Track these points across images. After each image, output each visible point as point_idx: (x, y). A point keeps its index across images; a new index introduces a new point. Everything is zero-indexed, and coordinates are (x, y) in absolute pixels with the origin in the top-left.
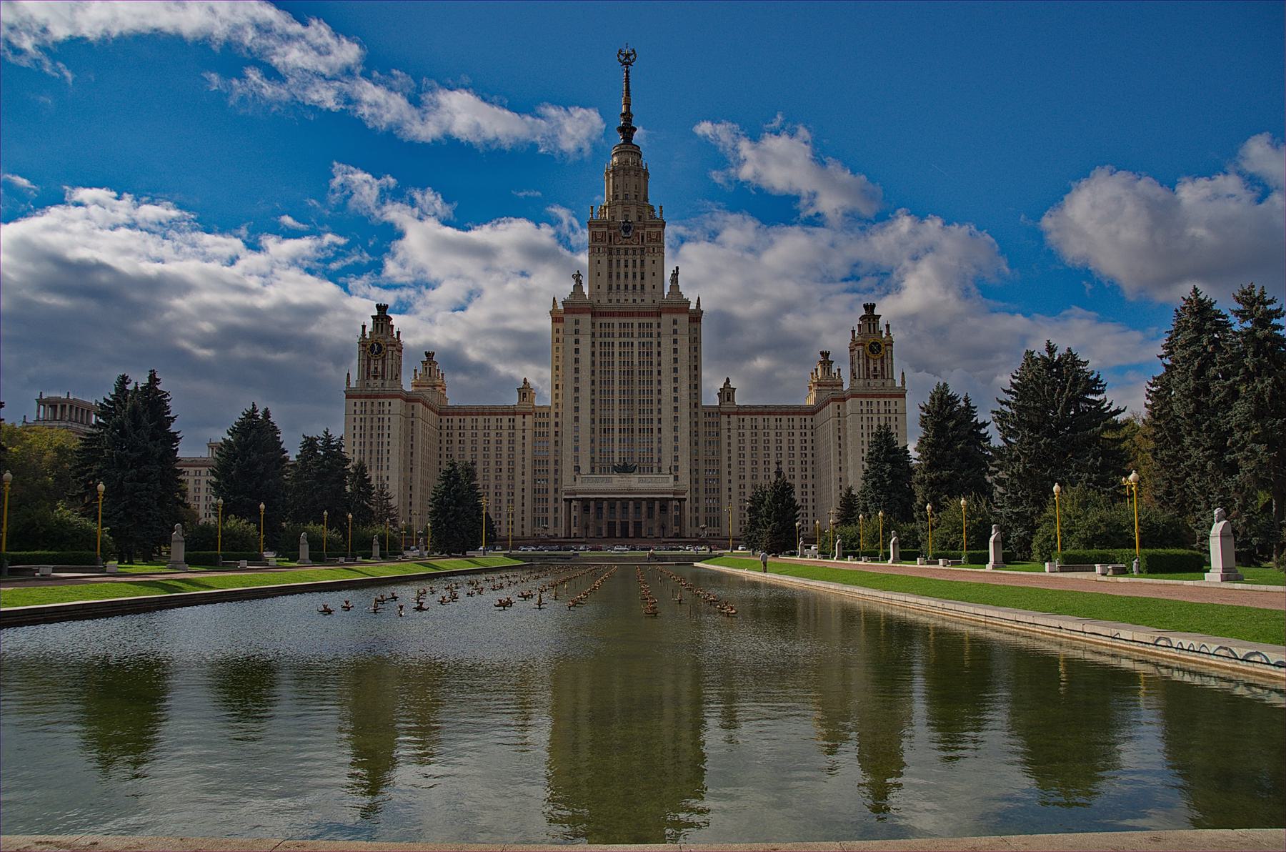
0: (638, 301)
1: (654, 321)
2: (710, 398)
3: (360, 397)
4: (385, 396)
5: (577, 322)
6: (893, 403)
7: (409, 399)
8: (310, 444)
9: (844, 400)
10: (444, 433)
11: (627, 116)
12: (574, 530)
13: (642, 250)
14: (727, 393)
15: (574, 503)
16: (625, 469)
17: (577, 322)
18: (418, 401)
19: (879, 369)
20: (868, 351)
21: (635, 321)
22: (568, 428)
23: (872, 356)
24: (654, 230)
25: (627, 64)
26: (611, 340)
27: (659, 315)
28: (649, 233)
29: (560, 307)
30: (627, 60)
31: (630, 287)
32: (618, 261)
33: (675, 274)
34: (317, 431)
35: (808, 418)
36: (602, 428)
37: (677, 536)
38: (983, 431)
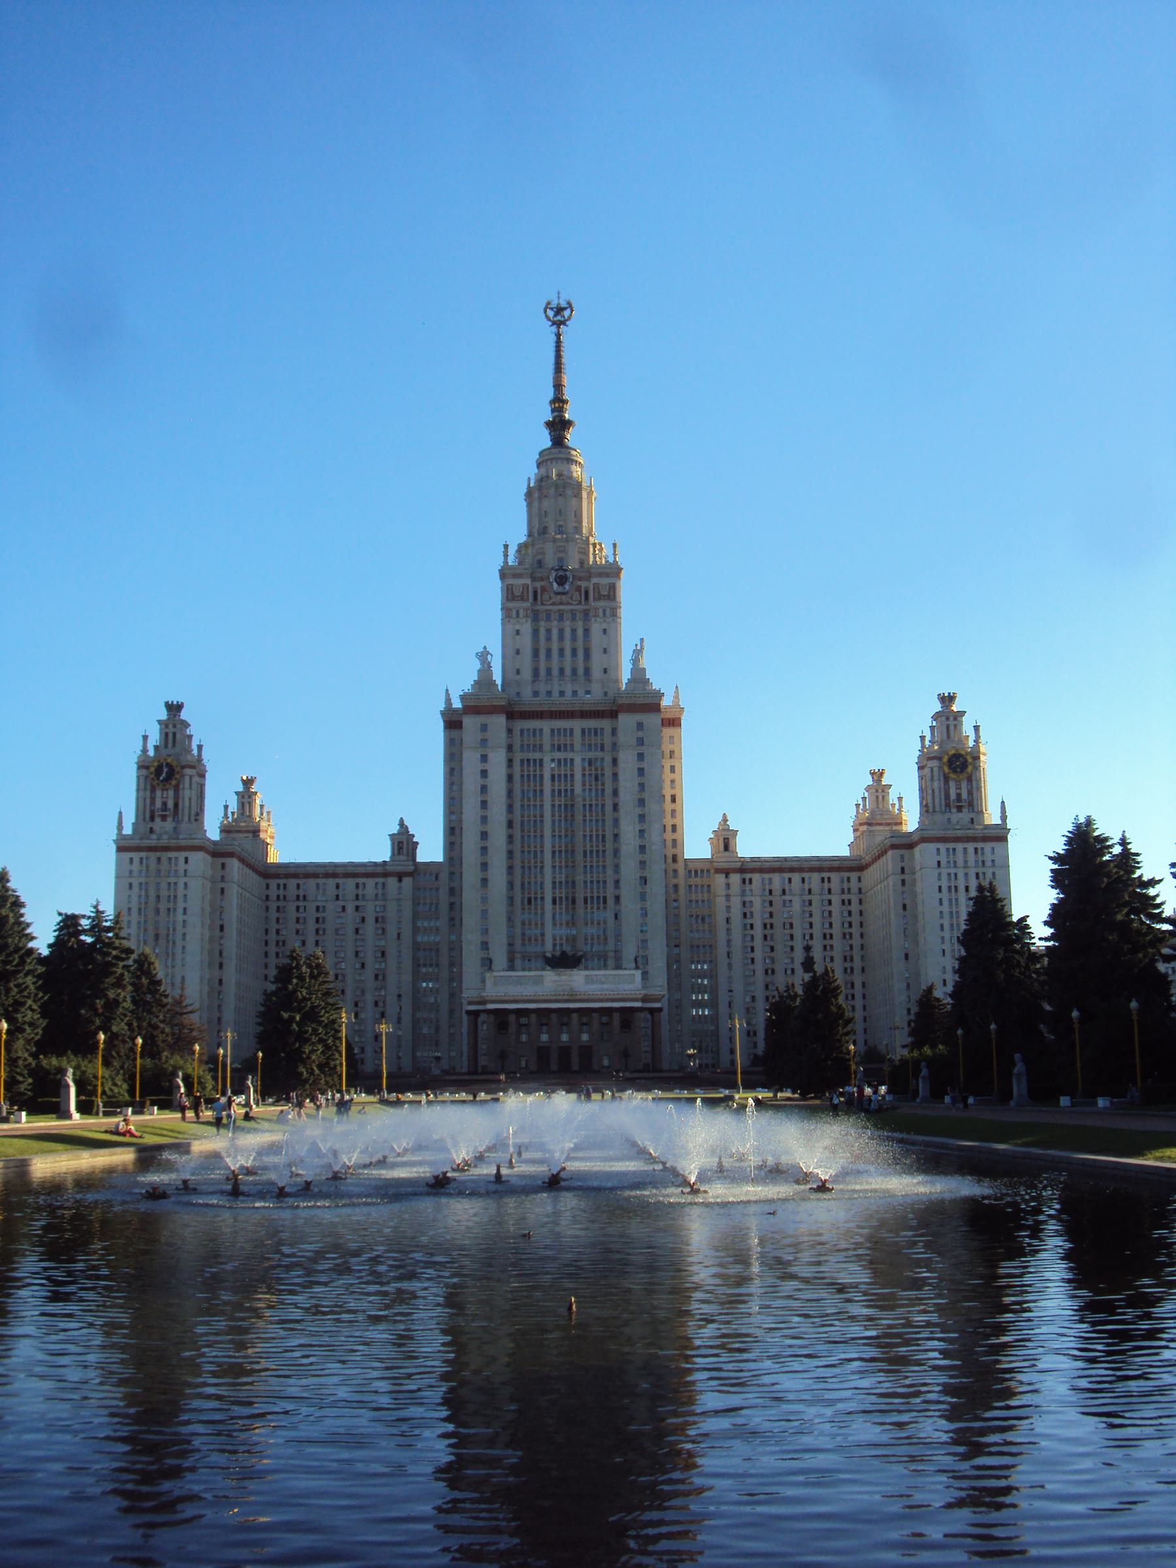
0: (581, 692)
1: (605, 724)
2: (697, 846)
3: (138, 849)
4: (180, 849)
5: (484, 728)
6: (988, 851)
7: (218, 852)
8: (69, 923)
9: (910, 846)
10: (273, 905)
11: (558, 402)
12: (483, 1061)
13: (586, 613)
14: (725, 839)
15: (483, 1017)
16: (564, 961)
17: (484, 728)
18: (231, 855)
19: (964, 795)
20: (946, 769)
21: (577, 725)
22: (470, 896)
23: (952, 776)
24: (604, 581)
25: (558, 324)
26: (537, 755)
27: (613, 714)
28: (596, 586)
29: (457, 704)
30: (559, 315)
31: (568, 672)
32: (549, 631)
33: (638, 653)
34: (82, 908)
35: (854, 876)
36: (524, 897)
37: (646, 1069)
38: (1152, 892)
